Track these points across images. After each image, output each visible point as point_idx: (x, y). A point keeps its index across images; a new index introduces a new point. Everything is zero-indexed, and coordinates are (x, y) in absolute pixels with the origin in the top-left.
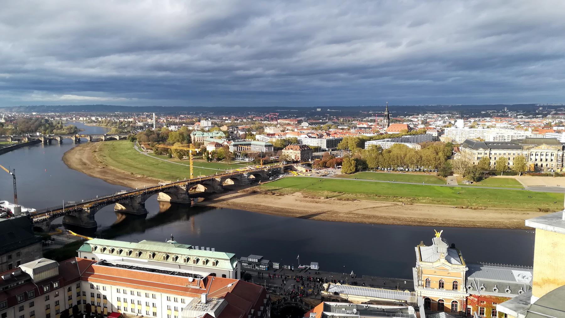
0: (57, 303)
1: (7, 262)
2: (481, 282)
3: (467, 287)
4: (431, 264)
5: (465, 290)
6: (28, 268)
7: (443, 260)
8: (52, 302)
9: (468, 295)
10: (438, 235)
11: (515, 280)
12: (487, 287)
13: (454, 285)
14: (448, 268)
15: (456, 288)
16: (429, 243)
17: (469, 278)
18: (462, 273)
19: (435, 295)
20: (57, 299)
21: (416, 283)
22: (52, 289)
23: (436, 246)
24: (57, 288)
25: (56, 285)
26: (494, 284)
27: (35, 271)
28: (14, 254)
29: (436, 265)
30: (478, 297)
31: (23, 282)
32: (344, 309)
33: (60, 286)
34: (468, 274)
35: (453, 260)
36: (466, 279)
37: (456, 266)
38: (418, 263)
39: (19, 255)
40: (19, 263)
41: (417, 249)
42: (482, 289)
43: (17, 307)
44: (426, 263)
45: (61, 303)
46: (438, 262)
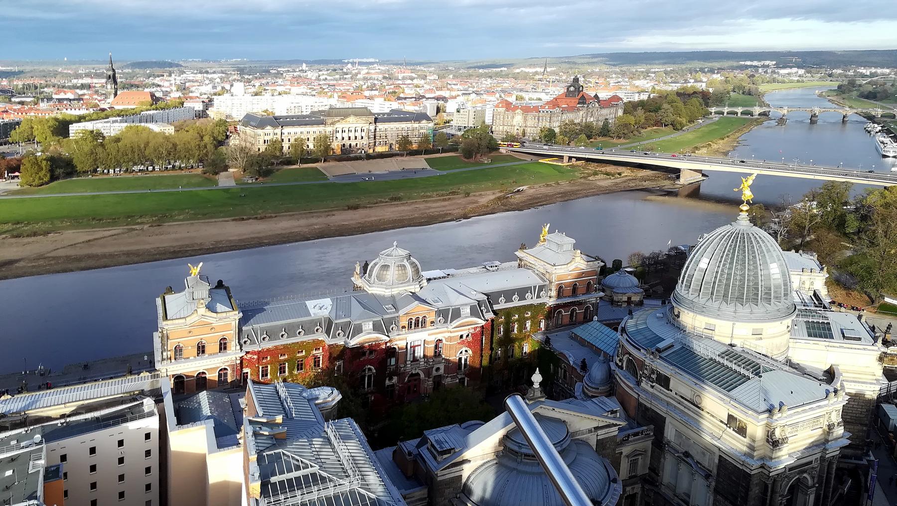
2: (262, 330)
3: (242, 342)
4: (183, 321)
5: (238, 347)
7: (202, 310)
9: (243, 354)
10: (195, 271)
11: (310, 315)
12: (271, 334)
13: (221, 344)
14: (210, 320)
15: (225, 348)
16: (181, 289)
17: (244, 328)
18: (233, 323)
19: (190, 367)
21: (158, 357)
23: (191, 290)
26: (280, 328)
29: (194, 318)
30: (259, 352)
32: (14, 443)
34: (242, 322)
35: (220, 307)
36: (240, 330)
37: (224, 315)
38: (162, 324)
41: (159, 301)
42: (264, 339)
44: (177, 321)
46: (195, 315)
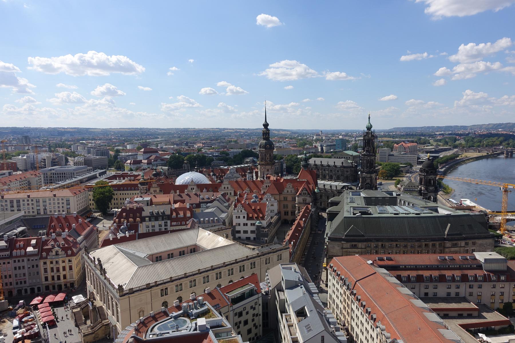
0: (502, 294)
1: (464, 247)
6: (481, 256)
8: (498, 290)
20: (502, 290)
22: (499, 280)
24: (503, 281)
25: (503, 278)
27: (485, 260)
28: (470, 242)
31: (475, 266)
33: (507, 280)
39: (474, 244)
40: (473, 251)
43: (468, 284)
45: (506, 295)
